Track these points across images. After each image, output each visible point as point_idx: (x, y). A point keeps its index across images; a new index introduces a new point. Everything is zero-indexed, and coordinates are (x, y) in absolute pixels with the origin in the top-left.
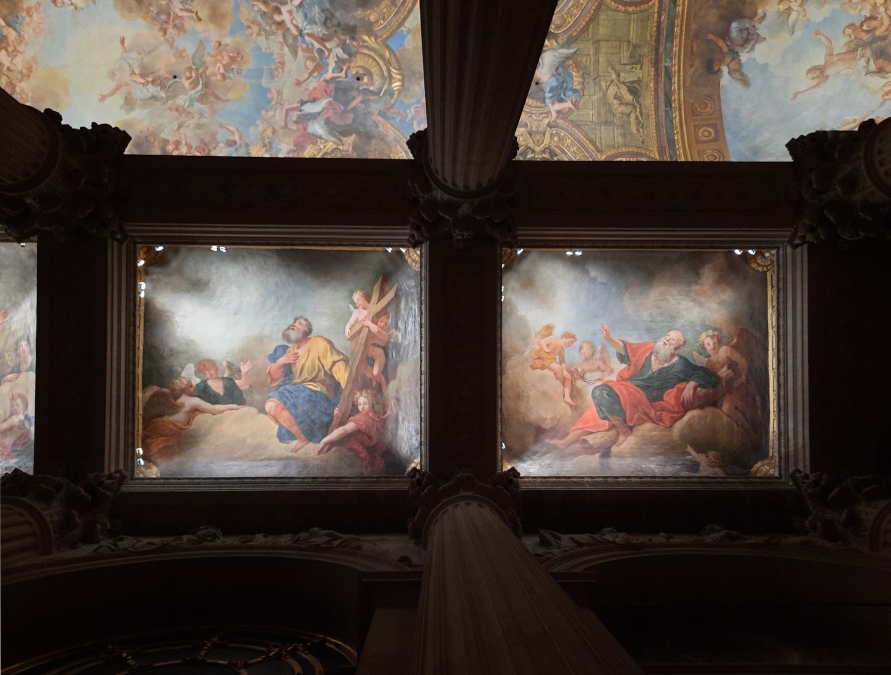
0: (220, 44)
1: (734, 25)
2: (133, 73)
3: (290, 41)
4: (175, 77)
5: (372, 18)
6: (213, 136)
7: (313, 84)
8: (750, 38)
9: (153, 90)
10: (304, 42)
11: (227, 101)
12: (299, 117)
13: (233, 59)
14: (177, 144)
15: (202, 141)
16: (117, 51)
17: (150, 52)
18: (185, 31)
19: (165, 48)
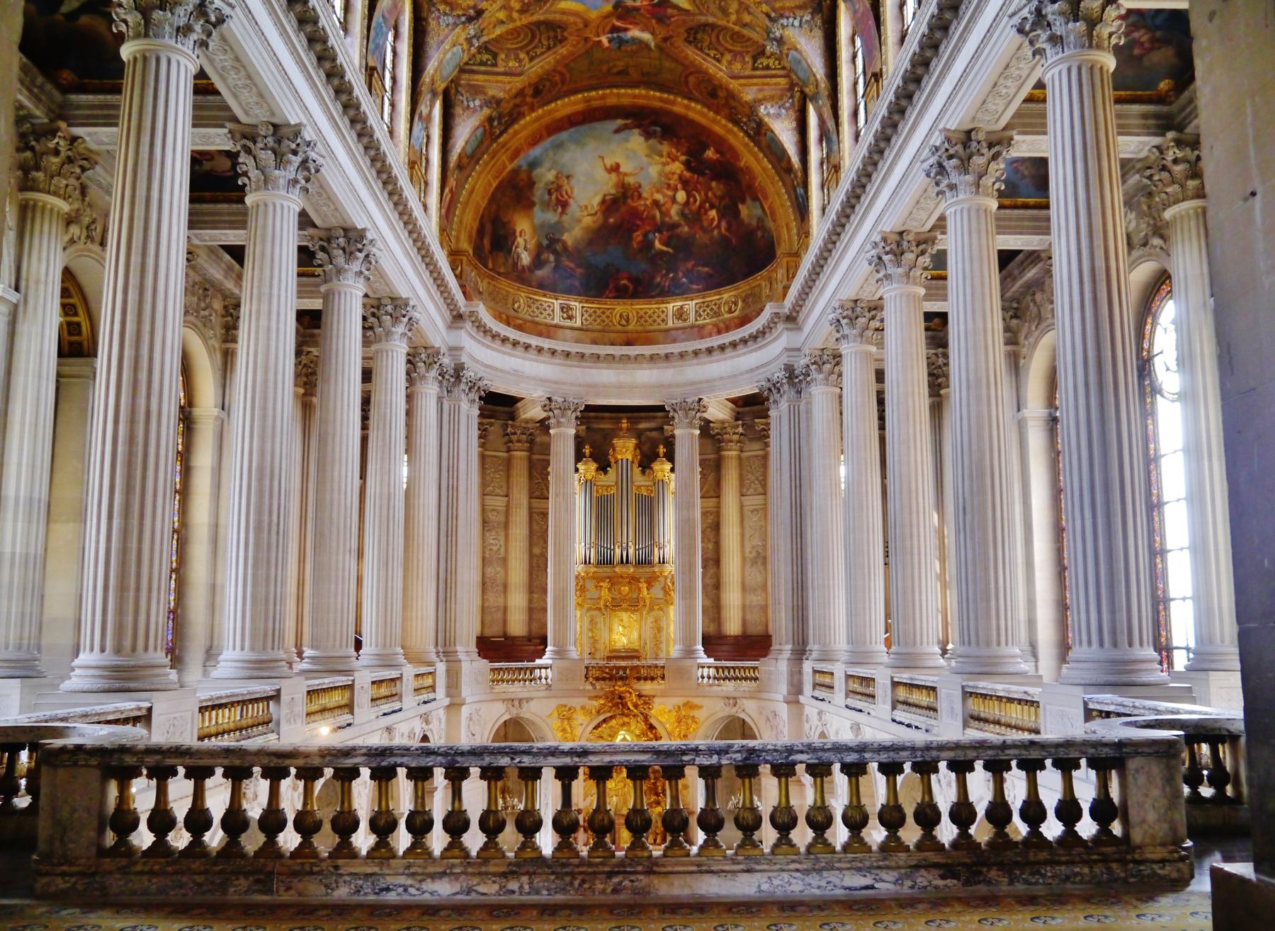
1: (658, 129)
8: (648, 135)
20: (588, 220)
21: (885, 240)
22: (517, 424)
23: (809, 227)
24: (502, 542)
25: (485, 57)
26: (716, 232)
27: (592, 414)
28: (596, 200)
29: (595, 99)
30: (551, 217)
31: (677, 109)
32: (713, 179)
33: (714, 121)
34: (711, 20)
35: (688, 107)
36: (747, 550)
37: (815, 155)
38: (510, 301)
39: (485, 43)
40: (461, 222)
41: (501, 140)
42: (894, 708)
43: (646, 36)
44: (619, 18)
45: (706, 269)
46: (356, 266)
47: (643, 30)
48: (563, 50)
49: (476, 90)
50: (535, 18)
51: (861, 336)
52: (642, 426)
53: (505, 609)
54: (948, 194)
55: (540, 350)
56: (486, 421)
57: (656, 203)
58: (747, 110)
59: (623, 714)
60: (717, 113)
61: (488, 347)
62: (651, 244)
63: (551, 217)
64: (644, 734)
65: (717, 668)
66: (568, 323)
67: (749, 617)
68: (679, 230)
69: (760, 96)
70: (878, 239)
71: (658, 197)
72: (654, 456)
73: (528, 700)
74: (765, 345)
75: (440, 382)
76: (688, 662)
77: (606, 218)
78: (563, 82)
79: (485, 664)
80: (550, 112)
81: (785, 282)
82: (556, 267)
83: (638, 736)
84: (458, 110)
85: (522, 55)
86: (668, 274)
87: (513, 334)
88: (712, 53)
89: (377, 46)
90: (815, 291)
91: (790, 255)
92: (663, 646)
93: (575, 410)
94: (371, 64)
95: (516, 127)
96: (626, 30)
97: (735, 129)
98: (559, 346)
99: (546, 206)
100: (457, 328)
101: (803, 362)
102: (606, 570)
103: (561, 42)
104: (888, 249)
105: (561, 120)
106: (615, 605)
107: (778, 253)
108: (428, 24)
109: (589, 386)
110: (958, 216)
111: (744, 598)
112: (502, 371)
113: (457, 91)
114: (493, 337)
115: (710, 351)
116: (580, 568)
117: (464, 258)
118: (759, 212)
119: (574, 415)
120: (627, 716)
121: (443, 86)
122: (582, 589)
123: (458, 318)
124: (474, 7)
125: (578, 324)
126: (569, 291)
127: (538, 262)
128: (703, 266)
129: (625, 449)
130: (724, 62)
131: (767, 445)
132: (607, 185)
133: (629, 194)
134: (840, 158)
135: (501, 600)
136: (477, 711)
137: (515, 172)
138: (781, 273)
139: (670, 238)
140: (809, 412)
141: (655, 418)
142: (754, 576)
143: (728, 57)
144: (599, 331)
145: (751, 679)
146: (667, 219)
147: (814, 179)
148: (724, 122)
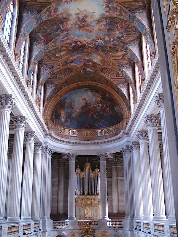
0: (94, 29)
1: (94, 90)
2: (86, 14)
3: (95, 40)
4: (85, 22)
5: (100, 51)
6: (70, 30)
7: (84, 43)
8: (92, 92)
9: (81, 18)
10: (94, 42)
11: (79, 30)
12: (76, 42)
13: (90, 31)
14: (67, 24)
15: (68, 29)
16: (91, 11)
17: (91, 17)
18: (97, 24)
19: (92, 20)
20: (78, 111)
21: (147, 116)
22: (61, 160)
23: (131, 112)
24: (57, 190)
25: (54, 75)
26: (109, 113)
27: (80, 157)
28: (80, 106)
29: (80, 84)
30: (70, 110)
31: (99, 86)
32: (108, 101)
33: (108, 88)
34: (106, 67)
35: (101, 85)
36: (119, 191)
37: (132, 96)
38: (59, 129)
39: (54, 73)
40: (48, 112)
41: (58, 93)
42: (154, 231)
43: (91, 70)
44: (85, 67)
45: (107, 122)
46: (23, 125)
47: (90, 69)
48: (72, 74)
49: (52, 83)
50: (65, 67)
51: (144, 138)
52: (93, 160)
53: (58, 206)
54: (160, 107)
55: (66, 142)
56: (52, 159)
57: (94, 106)
58: (115, 86)
60: (108, 86)
61: (54, 141)
62: (94, 116)
63: (70, 110)
66: (73, 135)
67: (120, 208)
68: (100, 113)
69: (118, 83)
70: (146, 116)
71: (94, 105)
73: (63, 230)
74: (121, 140)
75: (42, 150)
77: (83, 111)
78: (72, 80)
79: (52, 221)
80: (69, 87)
81: (126, 125)
82: (70, 122)
84: (48, 87)
85: (63, 75)
86: (98, 123)
87: (60, 138)
88: (107, 74)
89: (29, 75)
90: (133, 128)
91: (127, 119)
92: (98, 216)
93: (75, 156)
94: (28, 79)
95: (61, 90)
96: (87, 69)
97: (113, 90)
98: (71, 141)
99: (68, 108)
100: (46, 137)
101: (131, 144)
102: (83, 197)
103: (71, 72)
104: (148, 119)
105: (71, 89)
106: (86, 205)
107: (124, 118)
108: (41, 69)
109: (78, 150)
110: (163, 112)
112: (57, 147)
113: (47, 83)
114: (55, 139)
115: (108, 142)
116: (76, 196)
117: (48, 121)
118: (119, 109)
119: (75, 158)
120: (89, 235)
121: (44, 82)
122: (76, 201)
123: (46, 135)
124: (51, 66)
125: (76, 135)
126: (74, 128)
127: (66, 121)
128: (106, 121)
129: (88, 166)
130: (110, 75)
132: (83, 103)
133: (88, 104)
134: (137, 97)
135: (57, 204)
136: (50, 233)
137: (60, 100)
138: (125, 123)
139: (98, 115)
140: (133, 156)
143: (110, 74)
144: (81, 137)
146: (97, 110)
147: (132, 101)
148: (110, 88)
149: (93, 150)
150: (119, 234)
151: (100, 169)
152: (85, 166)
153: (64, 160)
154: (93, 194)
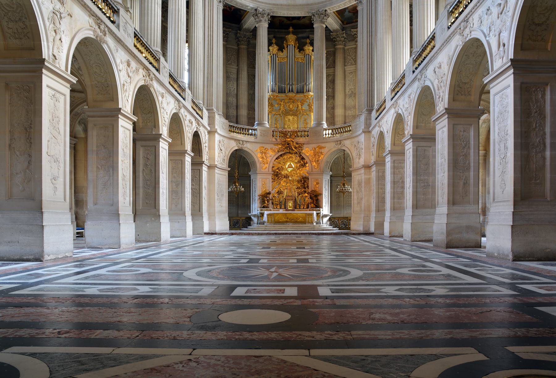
22: (242, 32)
36: (347, 91)
56: (227, 30)
59: (290, 153)
64: (299, 162)
65: (332, 130)
72: (305, 44)
76: (319, 128)
83: (296, 163)
93: (268, 15)
106: (287, 113)
109: (274, 4)
111: (345, 113)
116: (270, 93)
120: (292, 154)
122: (271, 105)
131: (356, 41)
135: (235, 113)
141: (306, 32)
142: (350, 102)
145: (348, 131)
149: (300, 5)
150: (344, 148)
151: (313, 47)
152: (286, 41)
153: (247, 34)
154: (301, 91)
